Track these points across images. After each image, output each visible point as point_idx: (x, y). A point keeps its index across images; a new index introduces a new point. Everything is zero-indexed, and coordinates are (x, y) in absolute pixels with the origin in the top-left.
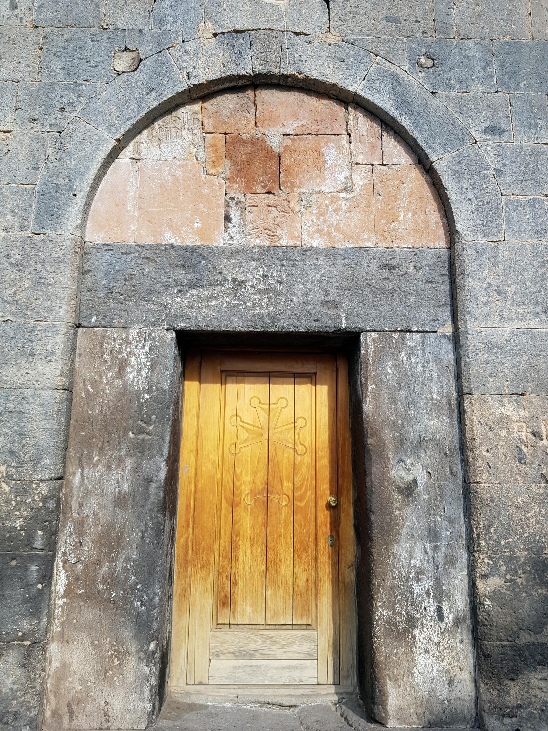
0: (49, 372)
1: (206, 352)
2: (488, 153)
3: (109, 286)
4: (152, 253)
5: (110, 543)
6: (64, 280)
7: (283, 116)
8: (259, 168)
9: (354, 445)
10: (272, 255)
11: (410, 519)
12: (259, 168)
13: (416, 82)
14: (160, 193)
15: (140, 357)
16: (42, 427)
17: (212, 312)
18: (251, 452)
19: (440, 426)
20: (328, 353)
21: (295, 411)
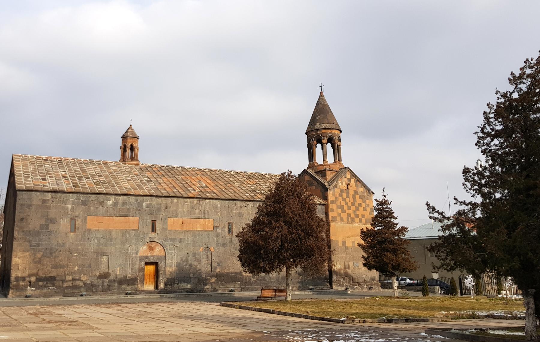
0: (138, 266)
1: (147, 264)
2: (168, 247)
3: (141, 259)
4: (144, 256)
5: (141, 278)
6: (138, 259)
7: (153, 245)
8: (151, 249)
9: (157, 271)
10: (152, 256)
11: (161, 276)
12: (151, 249)
13: (164, 241)
14: (143, 250)
15: (143, 265)
16: (137, 270)
17: (148, 261)
18: (149, 271)
19: (163, 269)
20: (156, 264)
21: (152, 268)
